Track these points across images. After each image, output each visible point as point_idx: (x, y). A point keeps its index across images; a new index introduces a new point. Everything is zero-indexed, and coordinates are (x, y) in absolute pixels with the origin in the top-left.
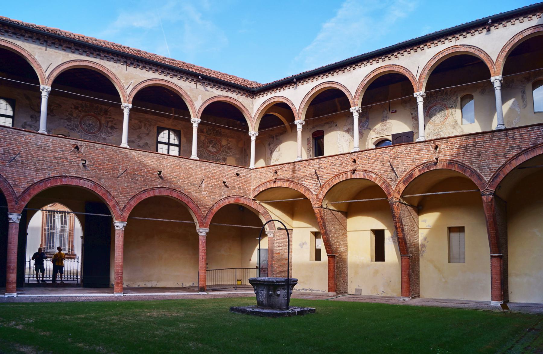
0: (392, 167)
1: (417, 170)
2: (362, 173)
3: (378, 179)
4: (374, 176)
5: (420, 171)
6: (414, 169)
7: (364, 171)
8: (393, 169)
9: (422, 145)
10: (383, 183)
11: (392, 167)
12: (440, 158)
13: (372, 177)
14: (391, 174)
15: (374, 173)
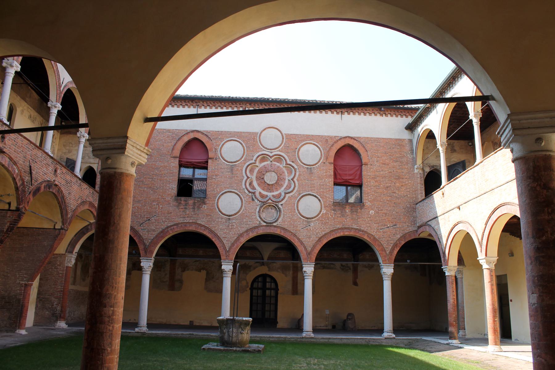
0: (31, 170)
1: (43, 185)
2: (8, 160)
3: (19, 177)
4: (17, 171)
5: (44, 187)
6: (41, 183)
7: (11, 159)
8: (31, 173)
9: (50, 161)
10: (21, 185)
11: (31, 170)
12: (56, 183)
13: (15, 171)
14: (27, 178)
15: (18, 168)
